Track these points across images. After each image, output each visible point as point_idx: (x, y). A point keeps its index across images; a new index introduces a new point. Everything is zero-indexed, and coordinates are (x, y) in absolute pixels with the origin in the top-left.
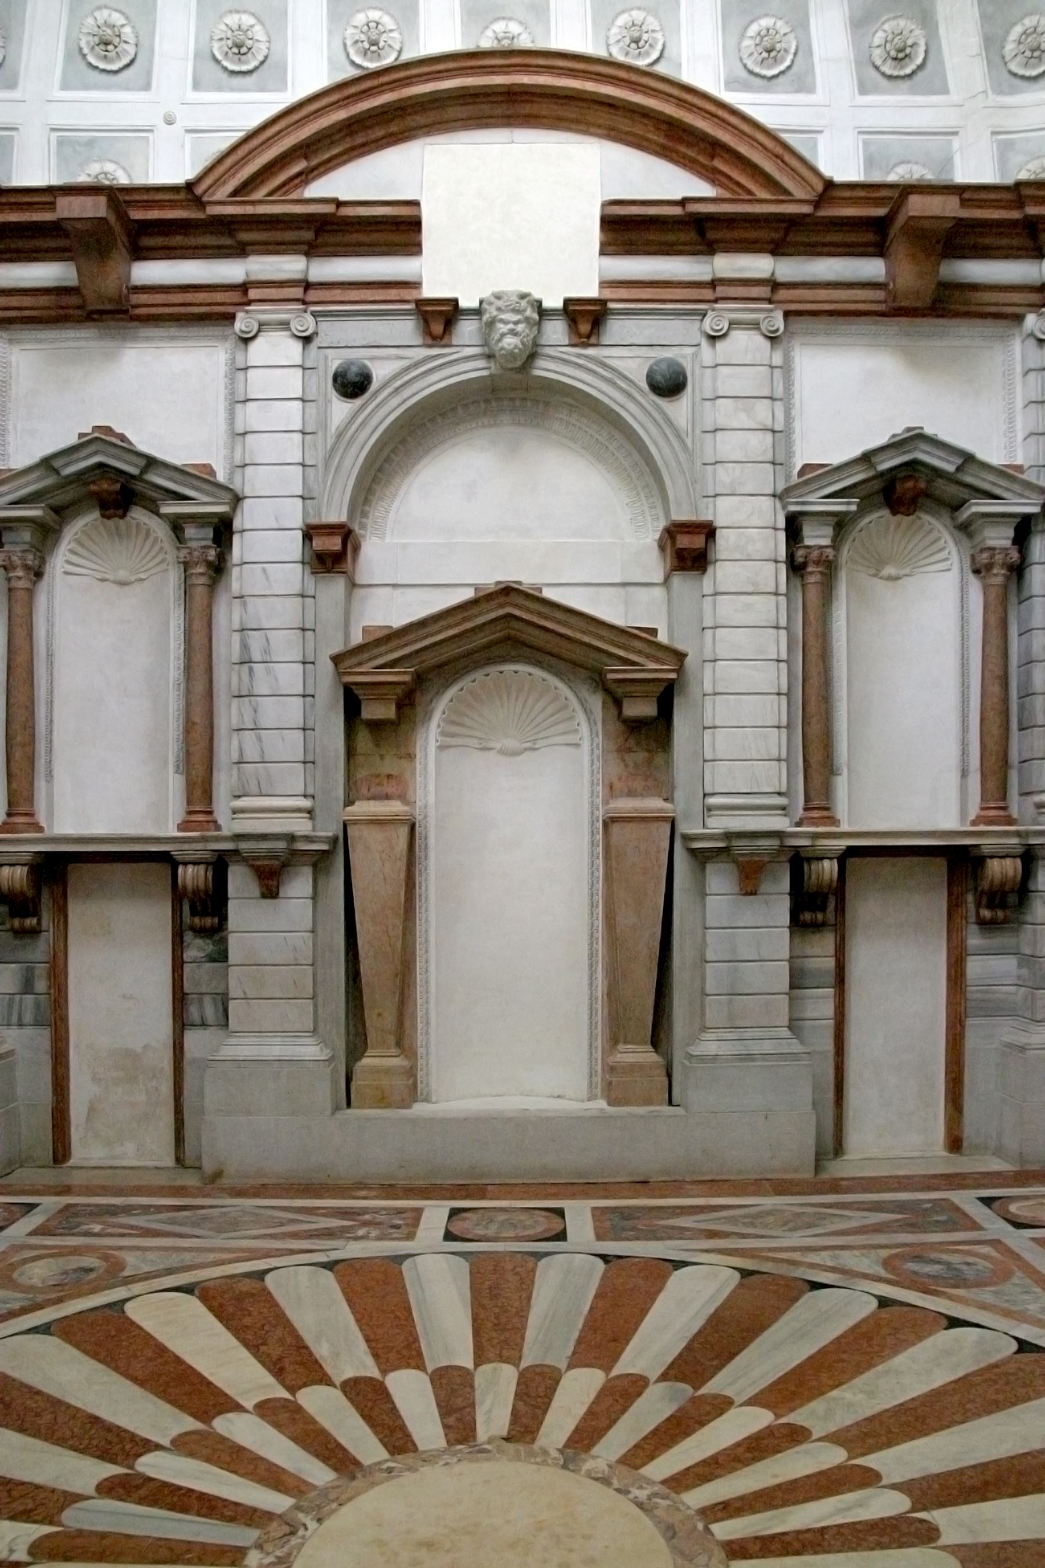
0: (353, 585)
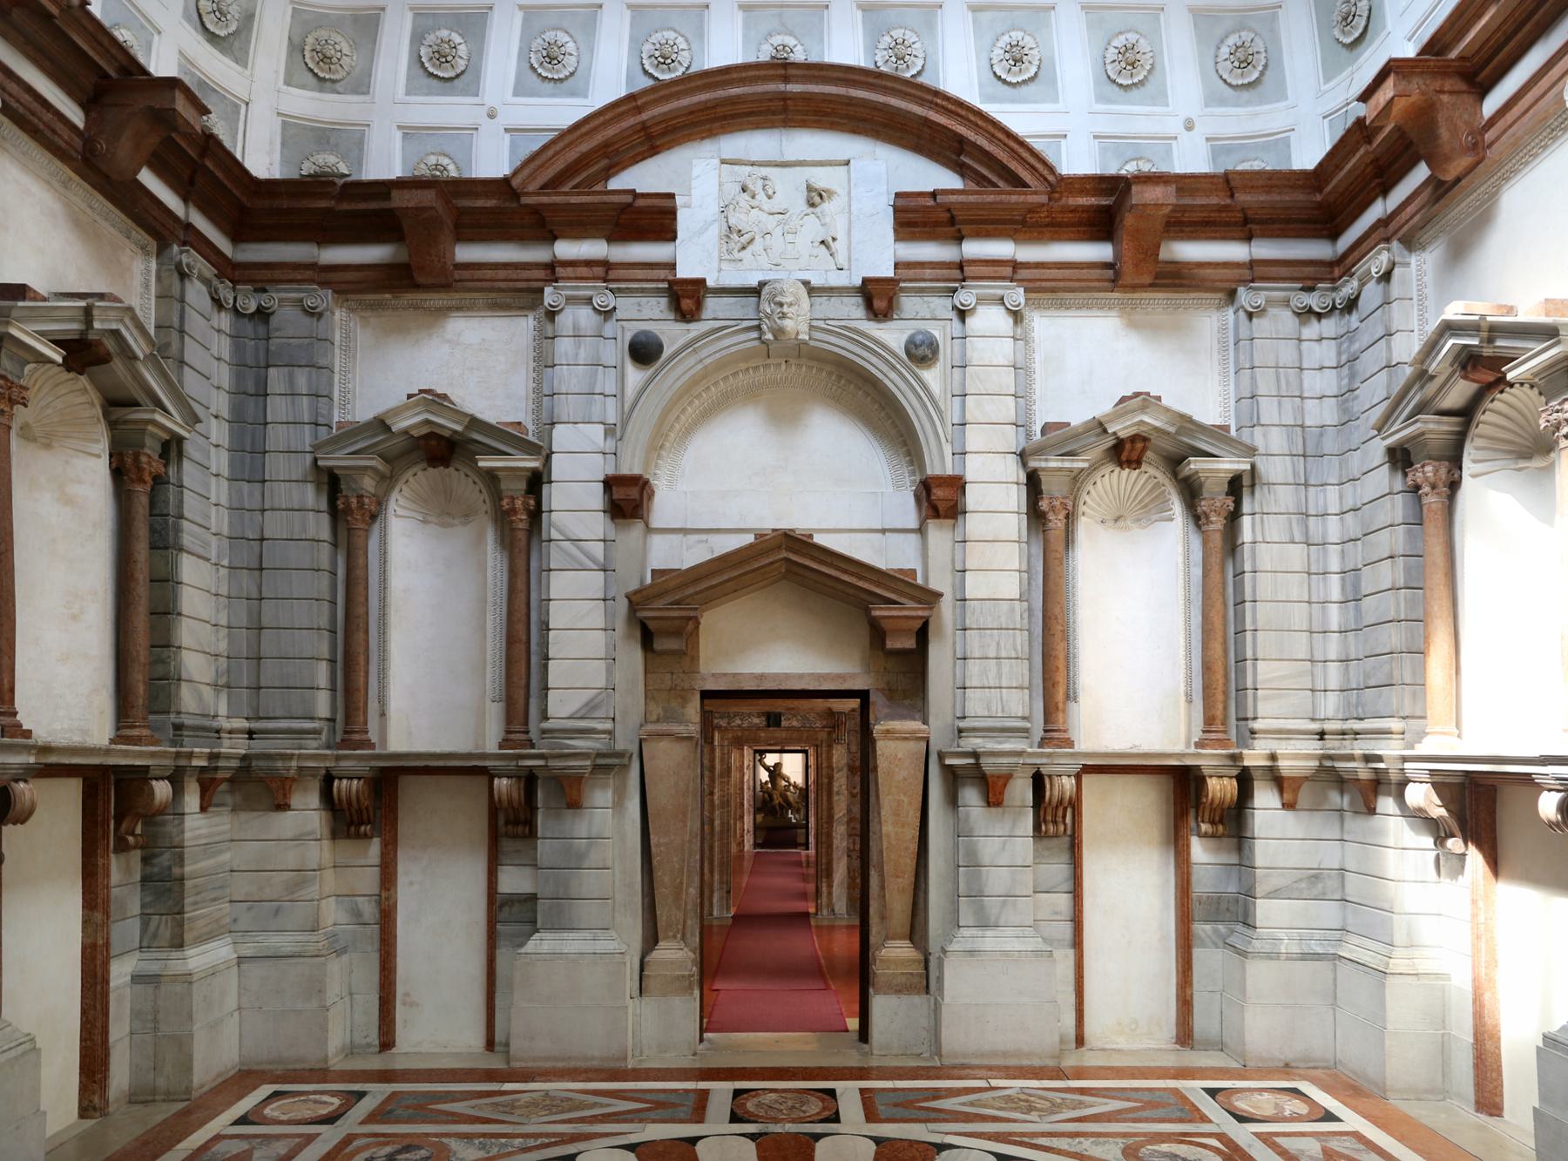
0: (649, 530)
